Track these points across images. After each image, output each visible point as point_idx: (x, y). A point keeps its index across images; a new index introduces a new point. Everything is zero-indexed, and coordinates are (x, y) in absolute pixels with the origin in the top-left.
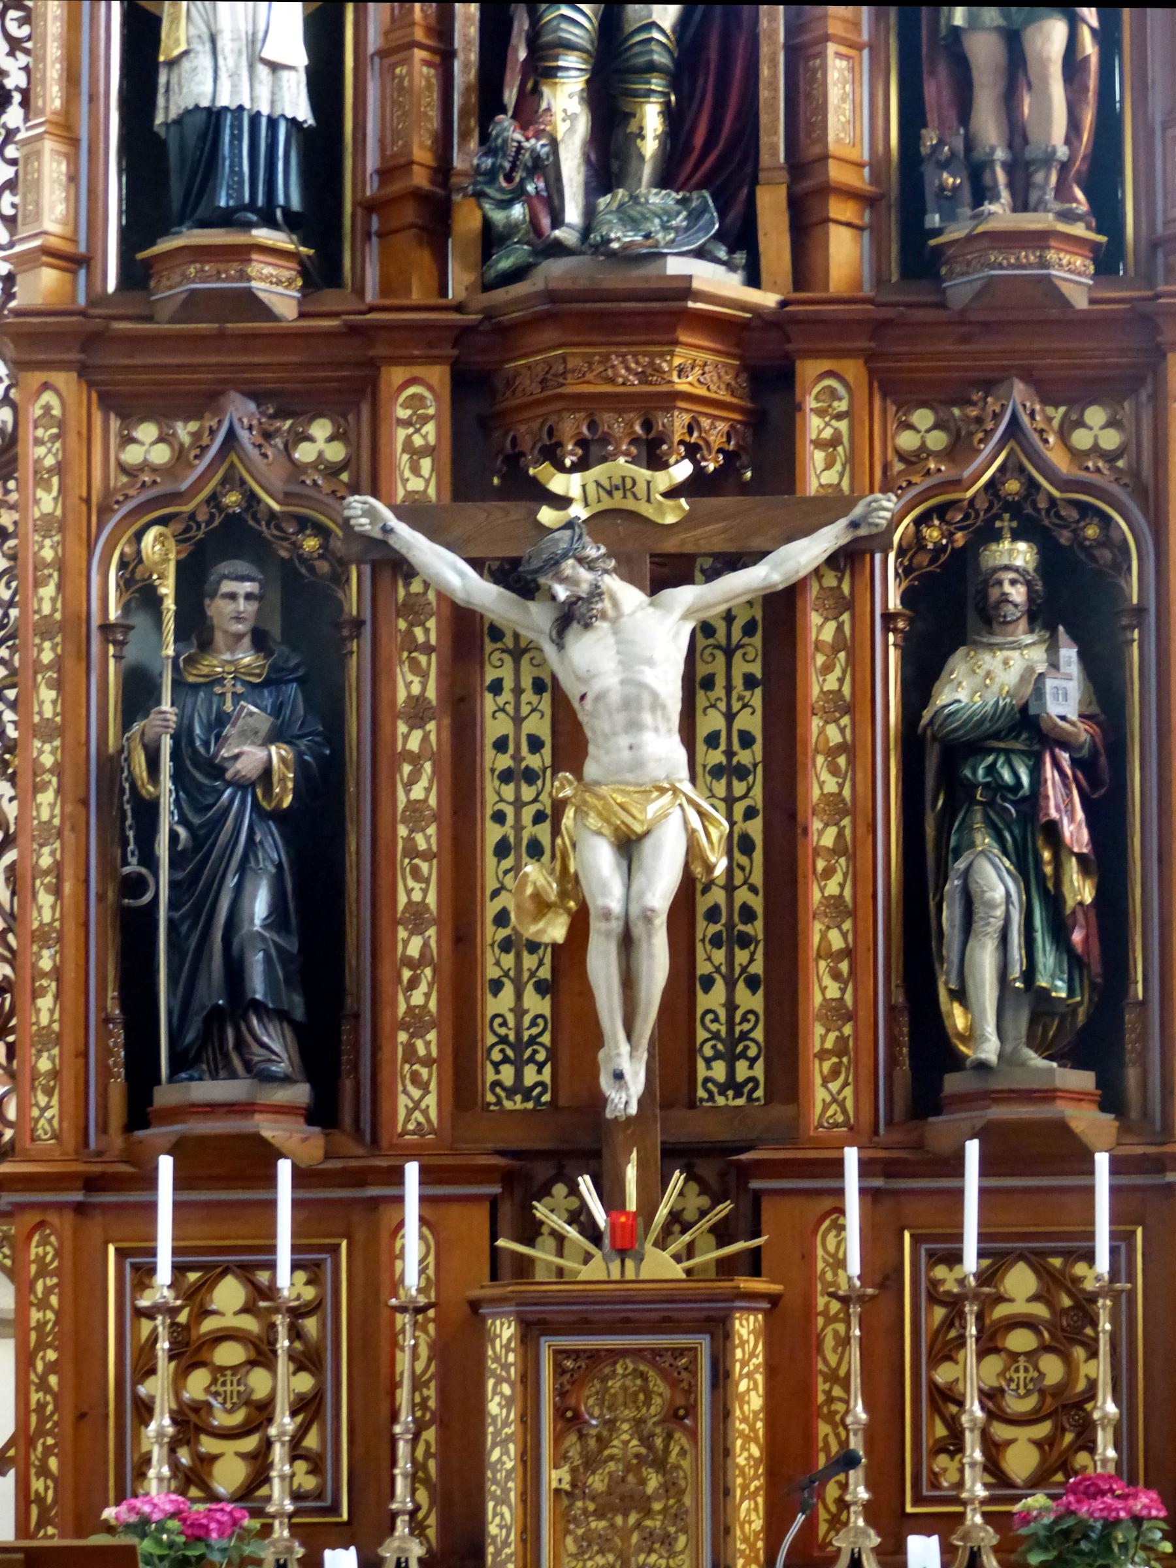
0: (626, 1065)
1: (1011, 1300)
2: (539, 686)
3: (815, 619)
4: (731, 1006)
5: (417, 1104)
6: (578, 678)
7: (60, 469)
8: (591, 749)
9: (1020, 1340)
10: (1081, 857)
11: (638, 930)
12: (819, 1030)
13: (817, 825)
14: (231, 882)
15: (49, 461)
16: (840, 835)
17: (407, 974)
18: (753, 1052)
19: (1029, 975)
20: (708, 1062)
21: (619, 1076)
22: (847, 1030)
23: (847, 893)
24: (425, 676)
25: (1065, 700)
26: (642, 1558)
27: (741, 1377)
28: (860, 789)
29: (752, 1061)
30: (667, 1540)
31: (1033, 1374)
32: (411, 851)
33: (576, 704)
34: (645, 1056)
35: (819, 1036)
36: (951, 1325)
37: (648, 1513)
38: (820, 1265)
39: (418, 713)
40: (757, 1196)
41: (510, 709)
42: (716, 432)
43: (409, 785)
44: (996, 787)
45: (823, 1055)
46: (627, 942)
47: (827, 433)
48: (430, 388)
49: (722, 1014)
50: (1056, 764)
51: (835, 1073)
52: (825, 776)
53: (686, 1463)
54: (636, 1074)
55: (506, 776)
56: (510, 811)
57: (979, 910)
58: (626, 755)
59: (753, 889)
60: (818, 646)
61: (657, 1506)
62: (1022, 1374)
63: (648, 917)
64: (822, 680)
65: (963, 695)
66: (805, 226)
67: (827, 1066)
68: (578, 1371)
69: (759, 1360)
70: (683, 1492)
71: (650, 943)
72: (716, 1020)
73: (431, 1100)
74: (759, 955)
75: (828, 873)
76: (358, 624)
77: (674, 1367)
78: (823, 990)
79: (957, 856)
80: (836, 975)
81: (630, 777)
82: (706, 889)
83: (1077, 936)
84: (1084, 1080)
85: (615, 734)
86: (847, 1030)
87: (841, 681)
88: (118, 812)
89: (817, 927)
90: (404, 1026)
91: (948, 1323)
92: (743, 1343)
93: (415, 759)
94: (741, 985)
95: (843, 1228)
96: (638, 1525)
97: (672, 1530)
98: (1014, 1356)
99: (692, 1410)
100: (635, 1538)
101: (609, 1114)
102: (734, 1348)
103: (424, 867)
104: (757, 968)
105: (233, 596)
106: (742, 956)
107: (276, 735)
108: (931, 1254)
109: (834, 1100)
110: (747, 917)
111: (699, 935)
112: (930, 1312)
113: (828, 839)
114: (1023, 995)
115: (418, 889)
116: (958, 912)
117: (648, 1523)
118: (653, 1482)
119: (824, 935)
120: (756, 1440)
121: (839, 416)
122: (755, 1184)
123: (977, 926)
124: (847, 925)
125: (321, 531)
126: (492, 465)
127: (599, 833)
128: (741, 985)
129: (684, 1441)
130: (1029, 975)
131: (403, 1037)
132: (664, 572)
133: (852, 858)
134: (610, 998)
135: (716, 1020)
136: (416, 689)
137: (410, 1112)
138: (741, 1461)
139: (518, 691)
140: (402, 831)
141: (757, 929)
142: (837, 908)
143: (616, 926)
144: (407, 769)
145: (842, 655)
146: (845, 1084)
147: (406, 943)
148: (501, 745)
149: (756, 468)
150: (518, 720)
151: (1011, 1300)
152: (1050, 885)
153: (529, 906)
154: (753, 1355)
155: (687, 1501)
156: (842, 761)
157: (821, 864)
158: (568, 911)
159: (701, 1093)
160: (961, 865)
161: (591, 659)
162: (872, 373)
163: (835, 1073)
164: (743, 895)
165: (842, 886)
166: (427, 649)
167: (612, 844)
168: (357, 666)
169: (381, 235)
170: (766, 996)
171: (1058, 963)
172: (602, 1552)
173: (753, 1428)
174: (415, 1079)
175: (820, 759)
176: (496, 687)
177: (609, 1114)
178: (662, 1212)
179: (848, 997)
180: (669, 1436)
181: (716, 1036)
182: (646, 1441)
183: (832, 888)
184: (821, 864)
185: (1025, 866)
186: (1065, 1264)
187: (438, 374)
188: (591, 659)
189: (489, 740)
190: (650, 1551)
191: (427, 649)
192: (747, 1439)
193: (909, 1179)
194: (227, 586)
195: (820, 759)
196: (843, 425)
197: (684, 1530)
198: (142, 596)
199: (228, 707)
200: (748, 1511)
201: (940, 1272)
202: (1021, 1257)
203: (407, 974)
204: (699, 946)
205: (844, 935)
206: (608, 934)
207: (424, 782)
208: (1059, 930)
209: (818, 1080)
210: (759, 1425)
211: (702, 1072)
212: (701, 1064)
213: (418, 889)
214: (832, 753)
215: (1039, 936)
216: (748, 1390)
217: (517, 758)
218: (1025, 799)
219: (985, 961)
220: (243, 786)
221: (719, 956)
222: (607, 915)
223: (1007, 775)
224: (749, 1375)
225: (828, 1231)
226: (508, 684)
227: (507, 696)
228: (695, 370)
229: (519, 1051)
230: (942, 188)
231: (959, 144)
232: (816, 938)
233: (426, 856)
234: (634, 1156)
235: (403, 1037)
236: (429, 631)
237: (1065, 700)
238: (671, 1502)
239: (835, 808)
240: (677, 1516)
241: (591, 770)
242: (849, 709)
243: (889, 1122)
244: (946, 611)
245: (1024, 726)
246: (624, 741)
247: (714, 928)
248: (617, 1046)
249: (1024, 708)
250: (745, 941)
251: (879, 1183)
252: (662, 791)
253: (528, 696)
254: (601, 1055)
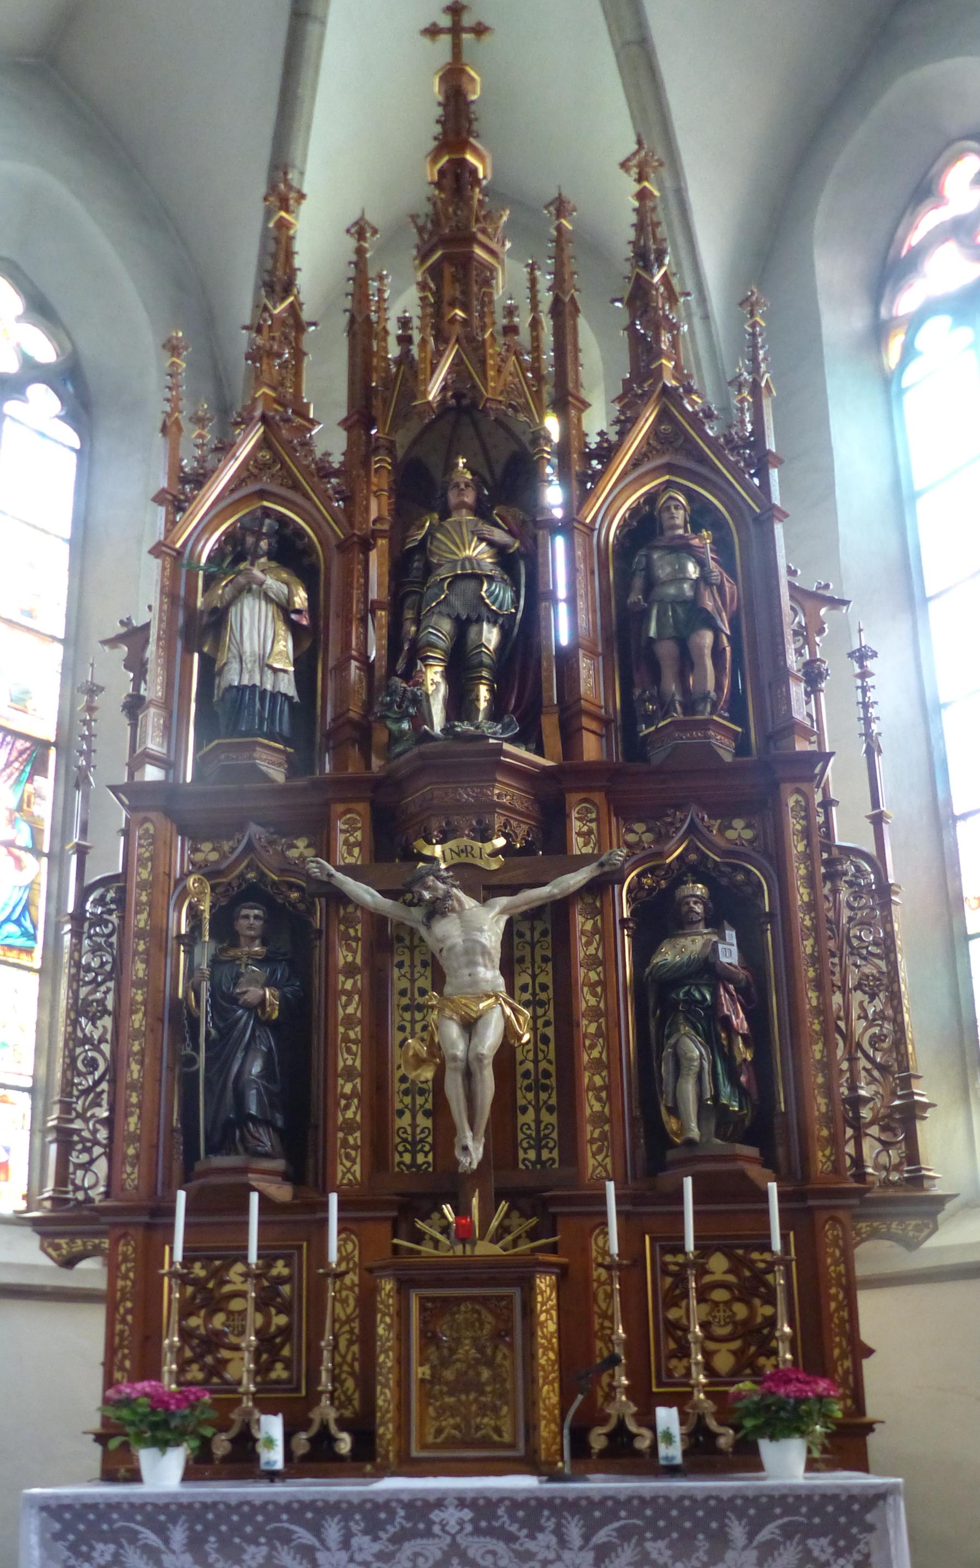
0: (470, 1143)
1: (713, 1273)
2: (424, 964)
3: (580, 919)
4: (538, 1121)
5: (349, 1170)
6: (438, 940)
7: (151, 859)
8: (448, 979)
9: (720, 1295)
10: (743, 1036)
11: (474, 1066)
12: (589, 1128)
13: (584, 1022)
14: (240, 1055)
15: (147, 855)
16: (599, 1027)
17: (343, 1102)
18: (551, 1144)
19: (716, 1097)
20: (525, 1150)
21: (465, 1149)
22: (607, 1128)
23: (604, 1056)
24: (354, 952)
25: (729, 954)
26: (478, 1420)
27: (542, 1312)
28: (609, 1002)
29: (551, 1150)
30: (496, 1410)
31: (729, 1313)
32: (346, 1039)
33: (437, 955)
34: (483, 1140)
35: (590, 1131)
36: (677, 1287)
37: (482, 1393)
38: (594, 1254)
39: (350, 970)
40: (554, 1216)
41: (408, 975)
42: (522, 830)
43: (345, 1007)
44: (691, 1002)
45: (592, 1141)
46: (469, 1075)
47: (585, 829)
48: (358, 814)
49: (533, 1125)
50: (727, 990)
51: (600, 1150)
52: (589, 997)
53: (507, 1363)
54: (477, 1149)
55: (406, 1008)
56: (408, 1025)
57: (684, 1062)
58: (467, 978)
59: (550, 1062)
60: (583, 933)
61: (488, 1389)
62: (722, 1314)
63: (480, 1058)
64: (583, 949)
65: (669, 957)
66: (570, 736)
67: (595, 1147)
69: (553, 1302)
70: (505, 1380)
71: (481, 1074)
72: (529, 1128)
73: (357, 1168)
74: (554, 1094)
75: (592, 1047)
76: (320, 931)
77: (501, 1308)
78: (591, 1107)
79: (669, 1036)
80: (599, 1099)
81: (469, 990)
82: (522, 1063)
83: (743, 1079)
84: (753, 1151)
85: (460, 968)
86: (607, 1128)
87: (597, 949)
88: (179, 1020)
89: (587, 1074)
90: (341, 1130)
91: (674, 1286)
92: (542, 1293)
93: (349, 994)
94: (543, 1111)
95: (606, 1234)
96: (476, 1400)
97: (498, 1403)
98: (716, 1304)
99: (509, 1332)
100: (474, 1408)
101: (460, 1170)
102: (536, 1295)
103: (354, 1047)
104: (553, 1101)
105: (247, 917)
106: (543, 1096)
107: (270, 982)
108: (662, 1248)
109: (600, 1165)
111: (519, 1085)
112: (663, 1280)
113: (592, 1029)
115: (349, 1058)
116: (671, 1064)
117: (483, 1399)
118: (486, 1374)
119: (591, 1079)
120: (552, 1349)
121: (591, 821)
122: (552, 1210)
123: (684, 1071)
124: (604, 1073)
125: (299, 888)
126: (392, 845)
127: (451, 1018)
128: (543, 1111)
129: (505, 1350)
130: (716, 1097)
131: (341, 1135)
133: (607, 1039)
134: (458, 1105)
135: (529, 1128)
136: (350, 959)
137: (344, 1174)
138: (542, 1361)
139: (412, 966)
140: (341, 1030)
141: (553, 1081)
142: (597, 1065)
143: (461, 1065)
144: (344, 998)
145: (597, 937)
146: (607, 1156)
147: (343, 1086)
148: (403, 993)
150: (413, 981)
151: (713, 1273)
152: (726, 1050)
153: (412, 1061)
154: (549, 1299)
155: (508, 1386)
156: (599, 989)
157: (587, 1042)
158: (435, 1064)
159: (521, 1166)
160: (672, 1041)
162: (609, 802)
163: (600, 1150)
164: (543, 1065)
165: (601, 1053)
166: (356, 939)
167: (459, 1025)
168: (318, 954)
169: (334, 748)
170: (558, 1116)
171: (733, 1092)
172: (453, 1416)
173: (550, 1342)
174: (348, 1156)
175: (586, 989)
176: (400, 965)
177: (460, 1170)
178: (495, 1223)
179: (607, 1110)
180: (496, 1348)
181: (529, 1137)
182: (481, 1350)
183: (595, 1054)
184: (587, 1042)
185: (710, 1040)
186: (746, 1253)
187: (363, 807)
189: (396, 992)
190: (484, 1415)
191: (356, 939)
192: (546, 1349)
193: (649, 1207)
194: (244, 912)
195: (586, 989)
196: (594, 825)
197: (506, 1403)
199: (243, 970)
200: (548, 1392)
201: (669, 1258)
202: (718, 1249)
203: (343, 1102)
204: (519, 1092)
205: (603, 1078)
206: (455, 1069)
207: (354, 1005)
208: (733, 1076)
209: (590, 1154)
210: (554, 1340)
211: (521, 1155)
212: (521, 1152)
213: (349, 1058)
214: (593, 986)
215: (721, 1077)
216: (546, 1320)
217: (412, 999)
218: (709, 1007)
219: (689, 1089)
220: (249, 1008)
221: (530, 1096)
222: (455, 1058)
223: (697, 995)
224: (547, 1311)
225: (599, 1235)
226: (407, 963)
227: (406, 969)
230: (646, 710)
231: (655, 692)
232: (586, 1080)
233: (355, 1042)
234: (477, 1194)
235: (341, 1135)
236: (358, 930)
238: (498, 1386)
239: (595, 1014)
240: (502, 1395)
241: (448, 989)
242: (601, 963)
243: (634, 1177)
246: (466, 972)
247: (526, 1082)
248: (464, 1132)
249: (706, 960)
250: (545, 1088)
251: (628, 1208)
252: (489, 997)
253: (418, 968)
254: (456, 1139)
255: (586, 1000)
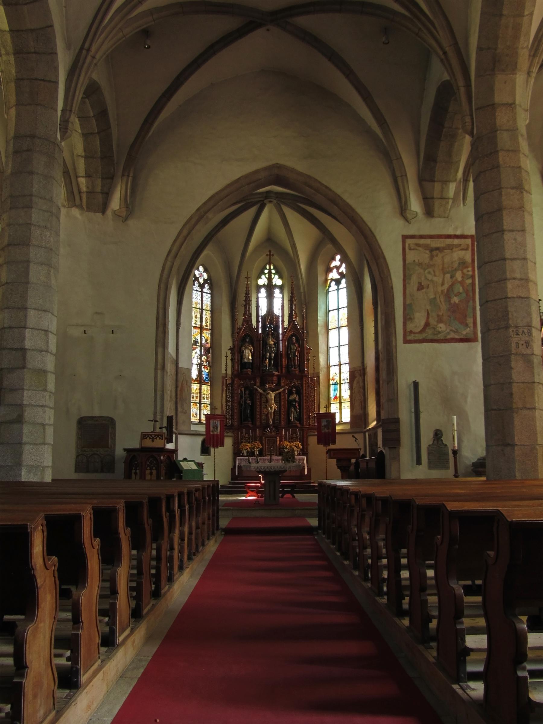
39: (258, 399)
42: (276, 382)
64: (282, 397)
68: (268, 440)
110: (278, 412)
114: (295, 417)
132: (273, 391)
149: (279, 386)
161: (269, 396)
185: (295, 409)
188: (269, 396)
198: (241, 391)
228: (275, 379)
229: (264, 420)
237: (297, 399)
244: (290, 393)
245: (294, 400)
255: (282, 404)
